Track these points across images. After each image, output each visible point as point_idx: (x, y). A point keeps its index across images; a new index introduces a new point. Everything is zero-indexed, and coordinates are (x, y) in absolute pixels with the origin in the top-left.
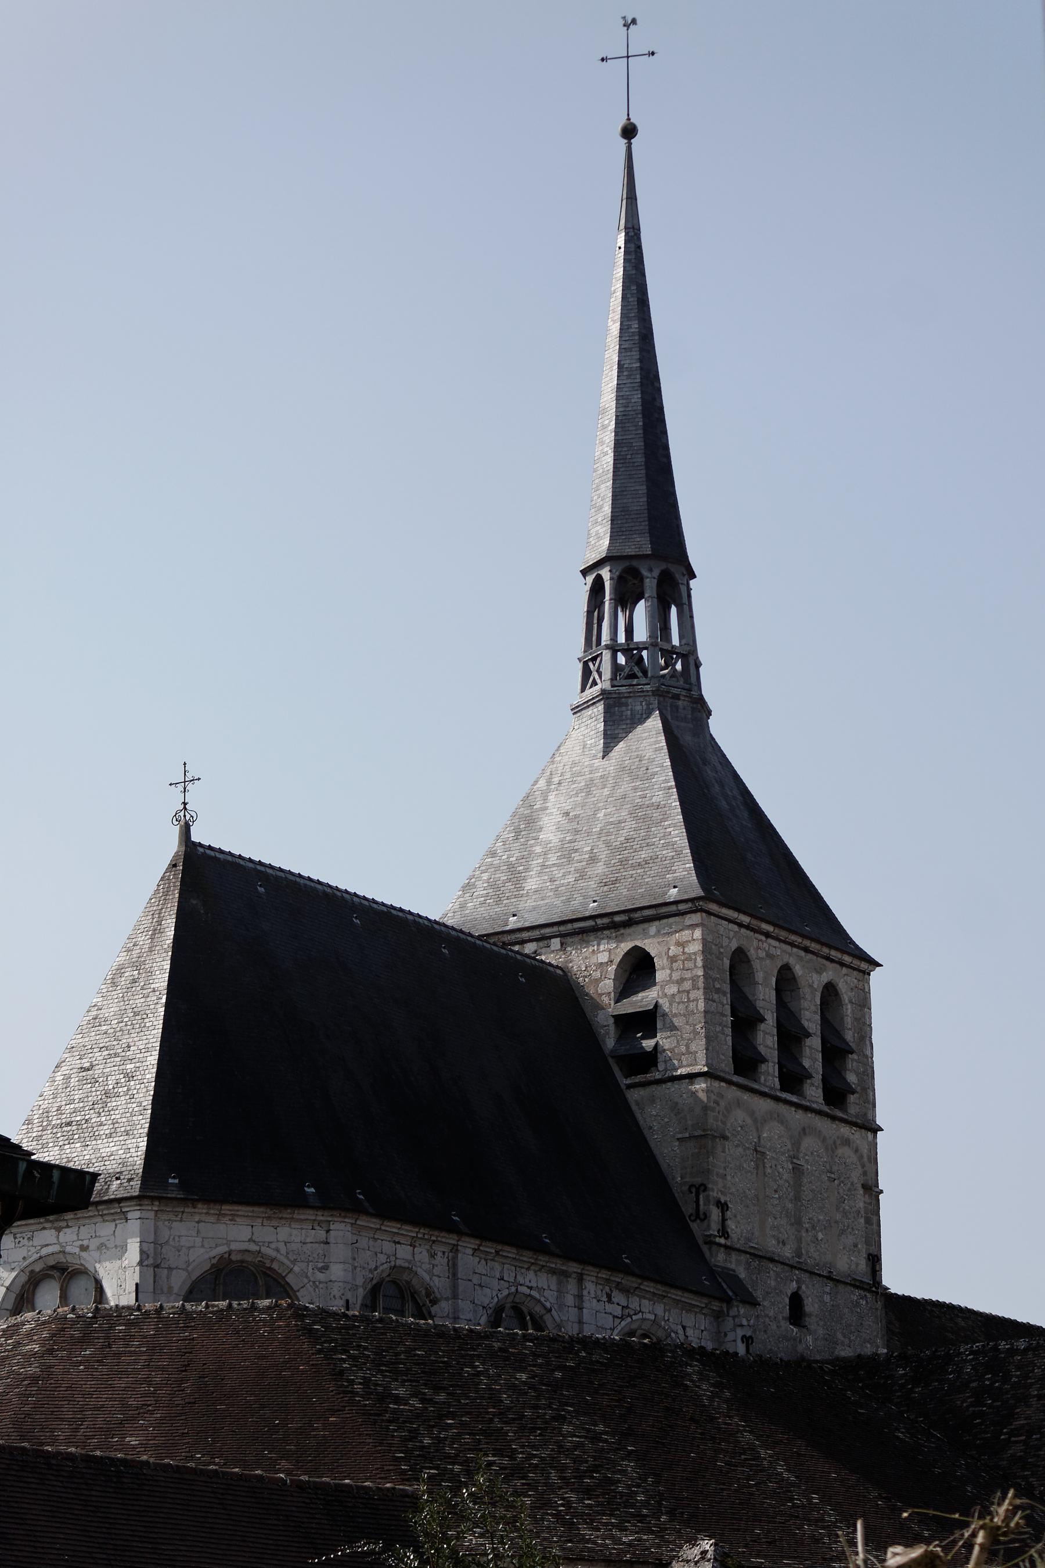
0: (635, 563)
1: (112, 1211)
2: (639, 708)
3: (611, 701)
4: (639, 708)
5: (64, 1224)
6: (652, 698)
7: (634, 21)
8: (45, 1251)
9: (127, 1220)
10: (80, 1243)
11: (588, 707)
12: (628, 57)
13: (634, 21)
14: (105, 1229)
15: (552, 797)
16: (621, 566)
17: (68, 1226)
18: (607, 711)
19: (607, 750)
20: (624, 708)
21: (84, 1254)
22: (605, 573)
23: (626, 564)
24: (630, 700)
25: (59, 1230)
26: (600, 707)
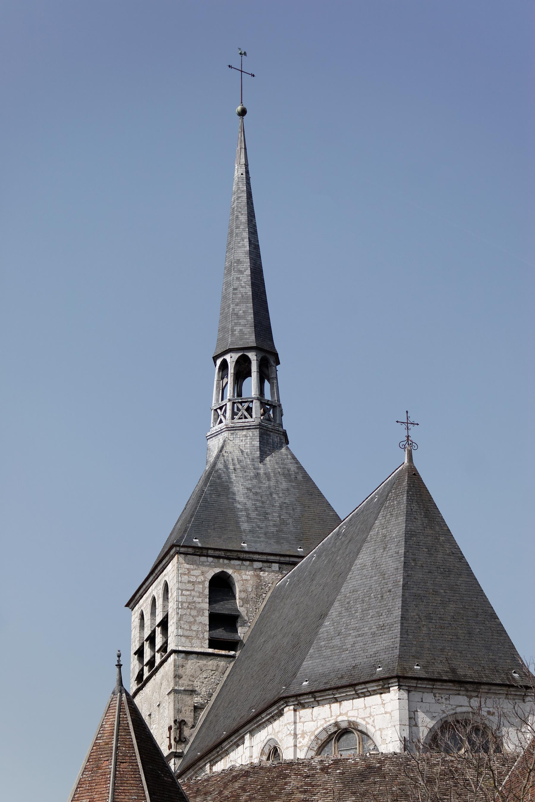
0: (268, 356)
1: (519, 693)
2: (276, 440)
3: (263, 431)
4: (276, 440)
5: (476, 694)
6: (282, 436)
7: (245, 54)
8: (459, 710)
9: (524, 701)
10: (488, 709)
11: (243, 429)
12: (242, 71)
13: (245, 54)
14: (507, 705)
15: (233, 476)
16: (261, 355)
17: (477, 696)
18: (261, 436)
19: (262, 459)
20: (268, 437)
21: (491, 717)
22: (252, 356)
23: (264, 354)
24: (272, 434)
25: (470, 697)
26: (257, 432)
